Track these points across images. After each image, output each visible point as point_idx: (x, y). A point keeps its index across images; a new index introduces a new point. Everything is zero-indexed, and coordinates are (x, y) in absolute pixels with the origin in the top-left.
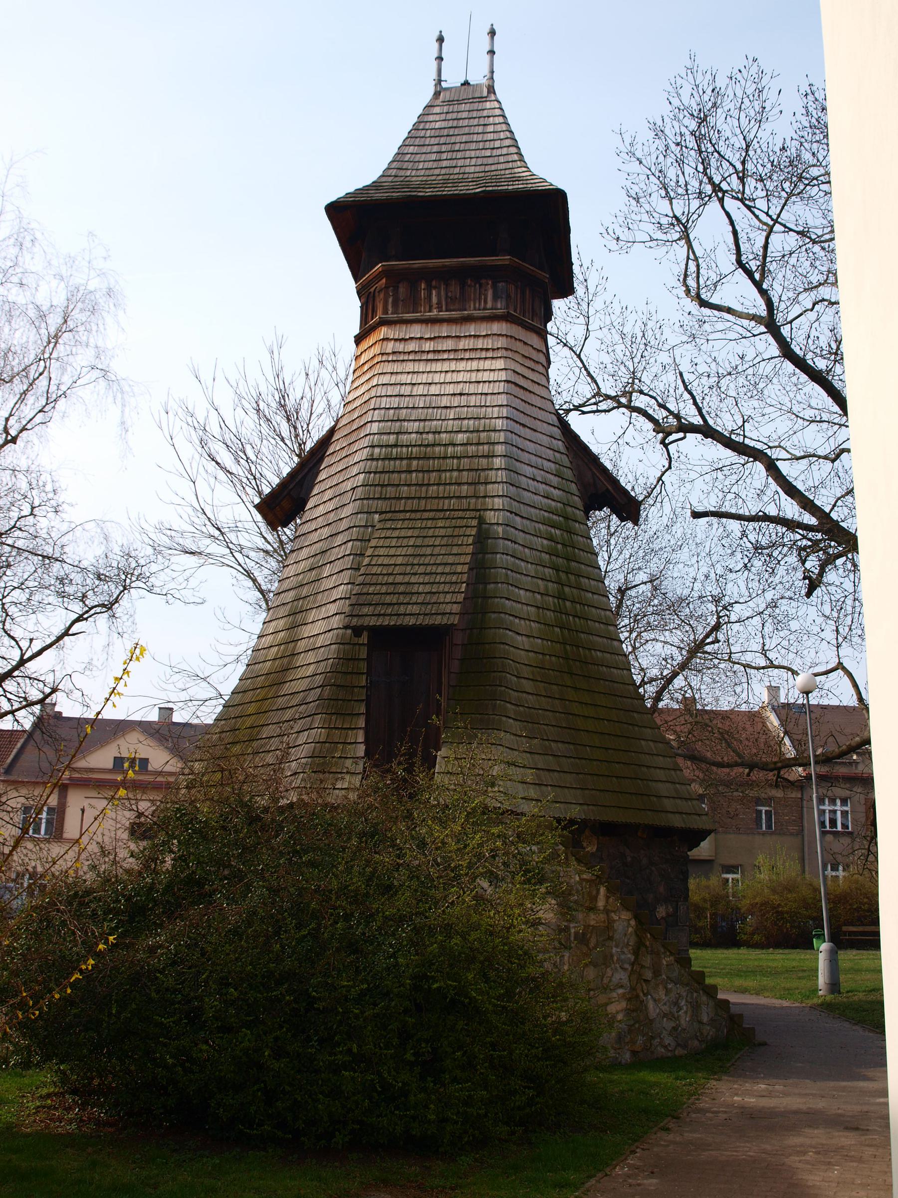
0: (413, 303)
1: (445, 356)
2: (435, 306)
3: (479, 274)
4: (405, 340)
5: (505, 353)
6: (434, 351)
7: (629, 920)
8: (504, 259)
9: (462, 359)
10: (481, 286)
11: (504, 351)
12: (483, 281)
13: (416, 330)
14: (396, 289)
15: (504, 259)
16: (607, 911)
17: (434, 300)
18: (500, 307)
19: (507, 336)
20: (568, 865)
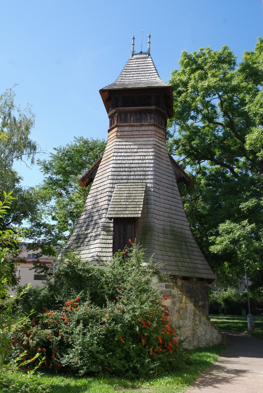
0: (125, 121)
1: (135, 136)
2: (132, 121)
3: (146, 112)
4: (124, 131)
5: (153, 136)
6: (132, 135)
8: (153, 107)
9: (140, 137)
10: (146, 115)
12: (147, 114)
13: (126, 129)
14: (121, 116)
15: (153, 107)
16: (186, 303)
17: (132, 119)
19: (154, 131)
20: (173, 289)
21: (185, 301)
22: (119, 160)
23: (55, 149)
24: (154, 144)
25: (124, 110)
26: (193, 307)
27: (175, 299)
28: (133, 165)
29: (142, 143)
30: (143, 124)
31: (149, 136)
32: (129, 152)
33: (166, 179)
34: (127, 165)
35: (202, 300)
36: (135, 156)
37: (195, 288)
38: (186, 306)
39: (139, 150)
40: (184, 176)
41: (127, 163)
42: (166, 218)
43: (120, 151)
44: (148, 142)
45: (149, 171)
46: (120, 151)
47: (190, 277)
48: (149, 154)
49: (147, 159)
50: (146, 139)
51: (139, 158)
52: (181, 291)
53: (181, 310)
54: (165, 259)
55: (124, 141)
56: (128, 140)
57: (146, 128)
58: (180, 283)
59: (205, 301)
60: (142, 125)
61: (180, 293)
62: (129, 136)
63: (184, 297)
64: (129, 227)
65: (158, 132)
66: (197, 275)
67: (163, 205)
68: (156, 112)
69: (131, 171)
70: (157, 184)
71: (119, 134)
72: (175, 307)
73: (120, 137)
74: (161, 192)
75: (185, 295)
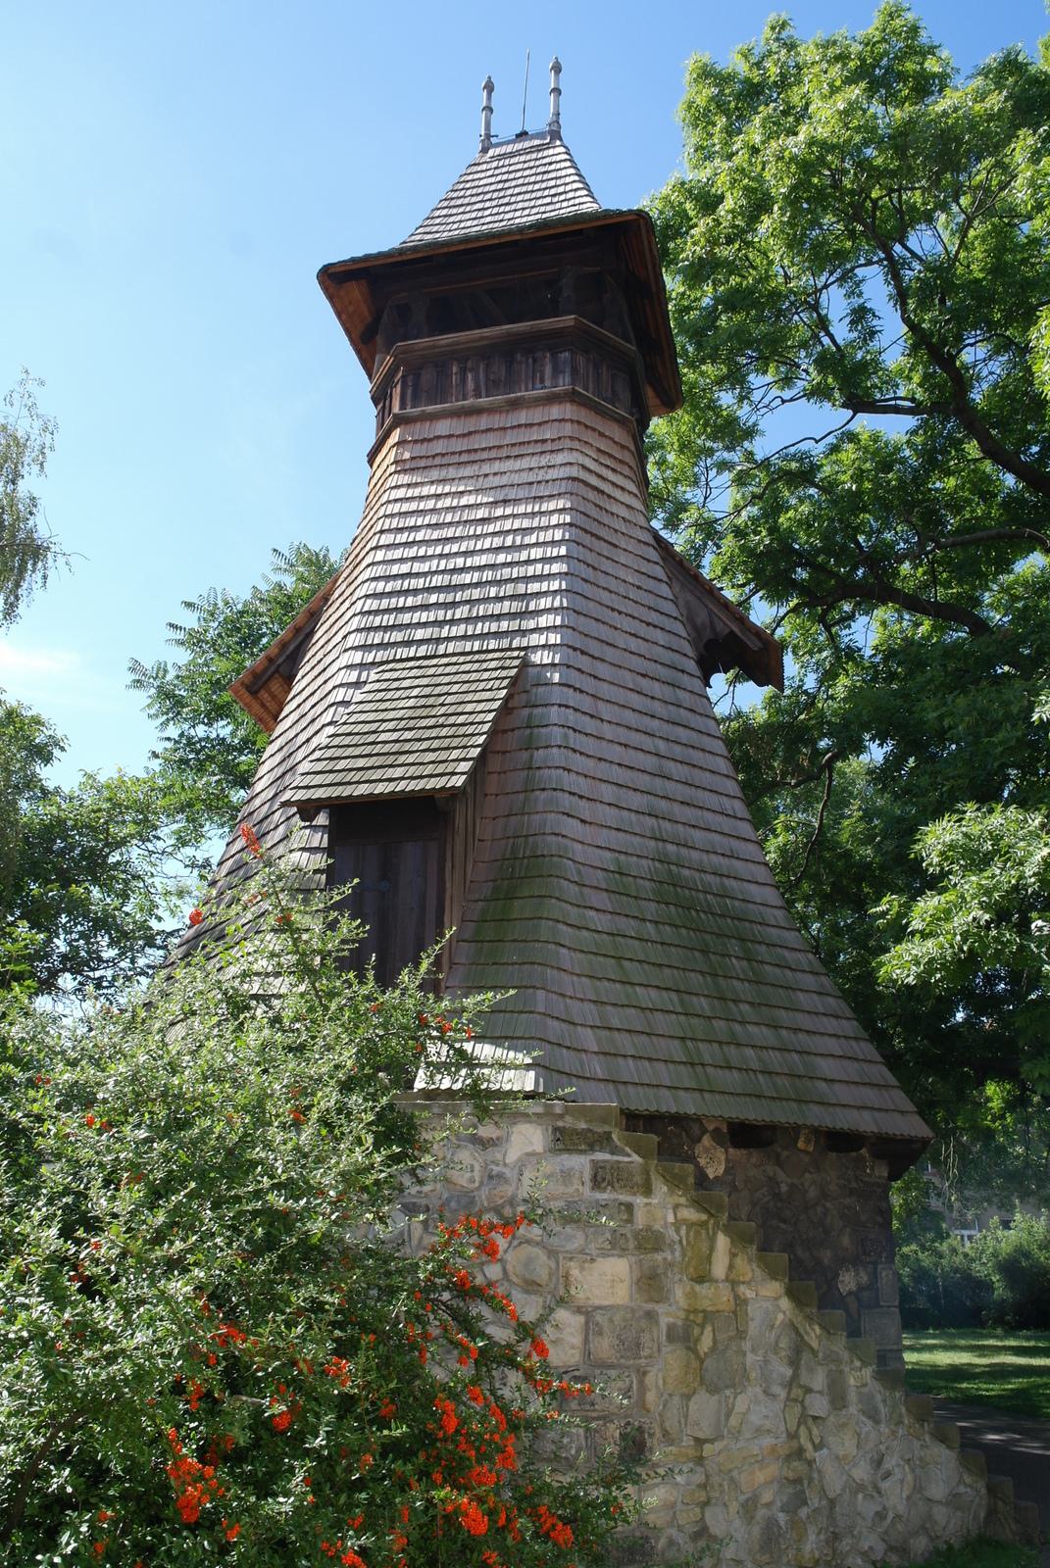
0: (439, 394)
1: (485, 455)
4: (429, 440)
5: (568, 444)
7: (776, 1299)
8: (568, 320)
9: (508, 457)
10: (535, 361)
11: (568, 441)
12: (539, 354)
13: (443, 427)
14: (418, 377)
15: (568, 320)
16: (734, 1283)
17: (470, 385)
18: (564, 384)
19: (572, 421)
20: (647, 1190)
21: (731, 1267)
22: (402, 560)
23: (189, 605)
24: (574, 479)
25: (434, 347)
26: (785, 1303)
27: (659, 1257)
28: (467, 578)
29: (516, 479)
30: (518, 398)
31: (548, 446)
32: (450, 524)
33: (634, 635)
34: (437, 580)
35: (856, 1262)
36: (477, 537)
37: (812, 1193)
38: (740, 1302)
39: (499, 512)
40: (736, 630)
41: (436, 572)
42: (633, 815)
43: (411, 522)
44: (542, 472)
45: (546, 593)
46: (411, 522)
47: (772, 1128)
48: (544, 521)
49: (537, 544)
50: (534, 462)
51: (497, 542)
52: (697, 1204)
53: (702, 1326)
54: (615, 1023)
55: (432, 482)
56: (452, 472)
57: (536, 415)
58: (714, 1162)
59: (875, 1264)
60: (515, 405)
61: (690, 1214)
62: (456, 459)
63: (722, 1241)
64: (410, 854)
65: (594, 430)
66: (817, 1117)
67: (616, 753)
68: (580, 341)
69: (454, 604)
70: (583, 653)
71: (407, 455)
72: (660, 1308)
73: (414, 464)
74: (605, 690)
75: (727, 1230)
